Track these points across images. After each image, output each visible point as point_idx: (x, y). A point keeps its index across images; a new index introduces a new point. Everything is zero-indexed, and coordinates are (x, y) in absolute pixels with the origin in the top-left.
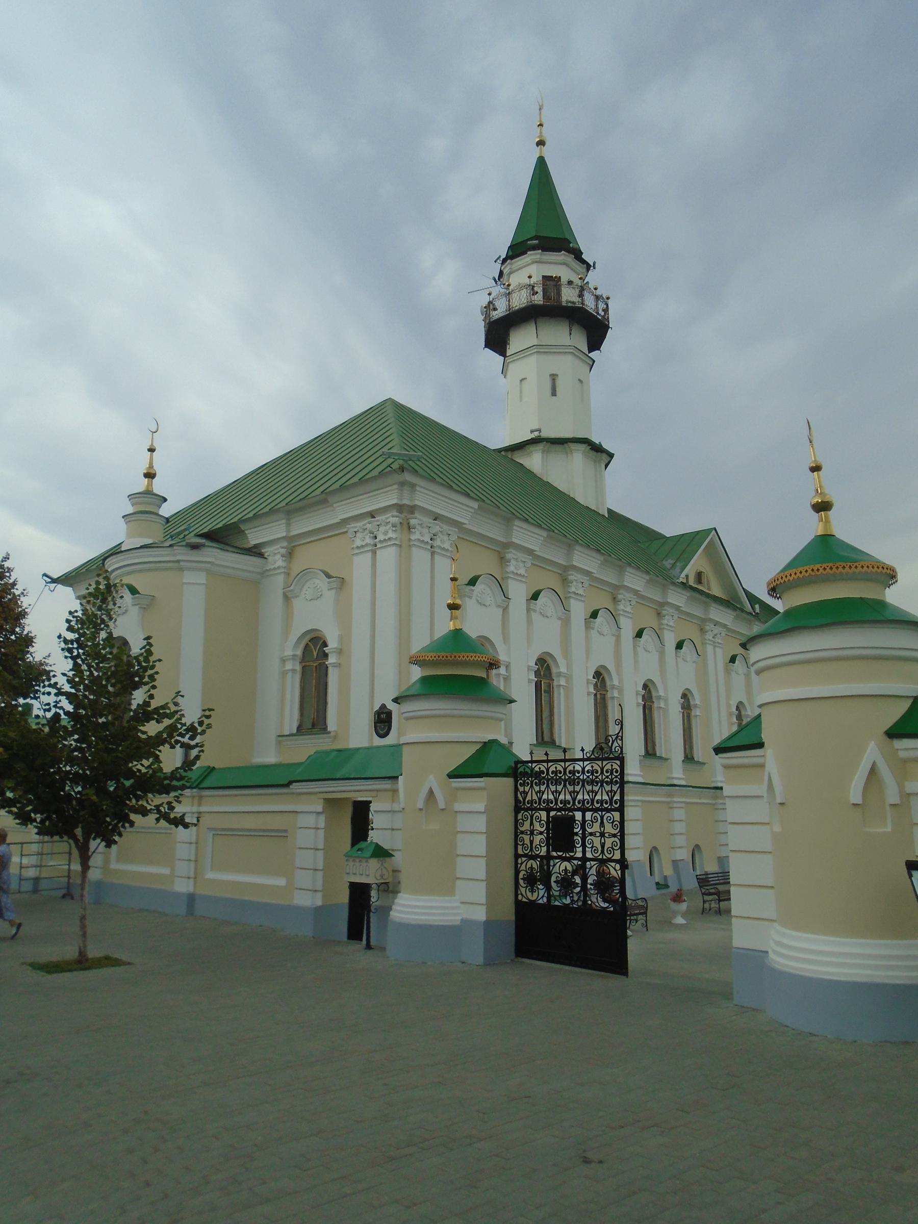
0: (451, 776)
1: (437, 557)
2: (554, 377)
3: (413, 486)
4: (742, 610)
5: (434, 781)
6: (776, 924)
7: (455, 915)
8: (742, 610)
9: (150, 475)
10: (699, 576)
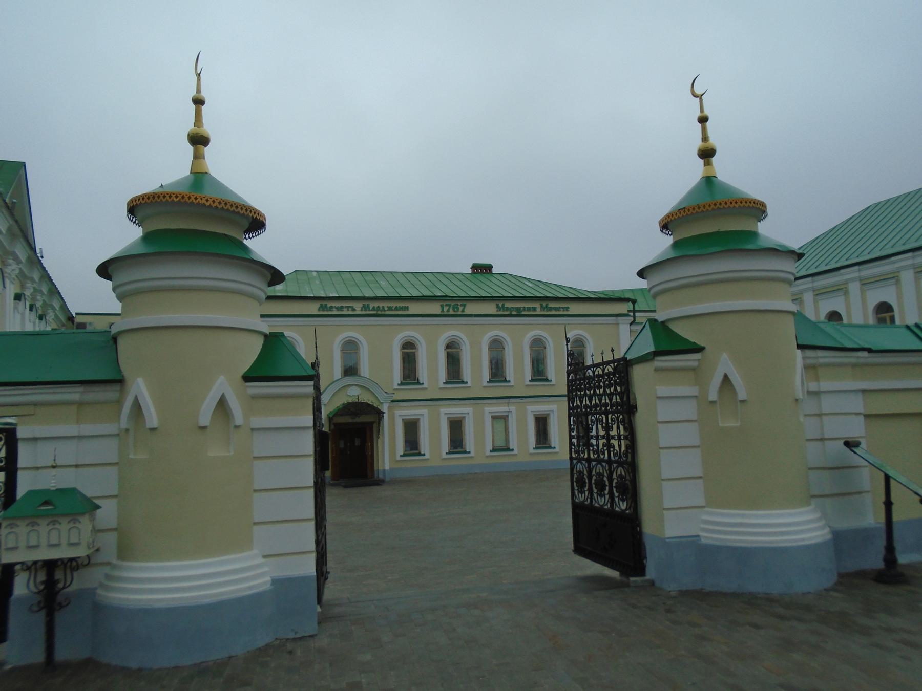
0: (247, 378)
5: (225, 385)
6: (706, 509)
7: (262, 575)
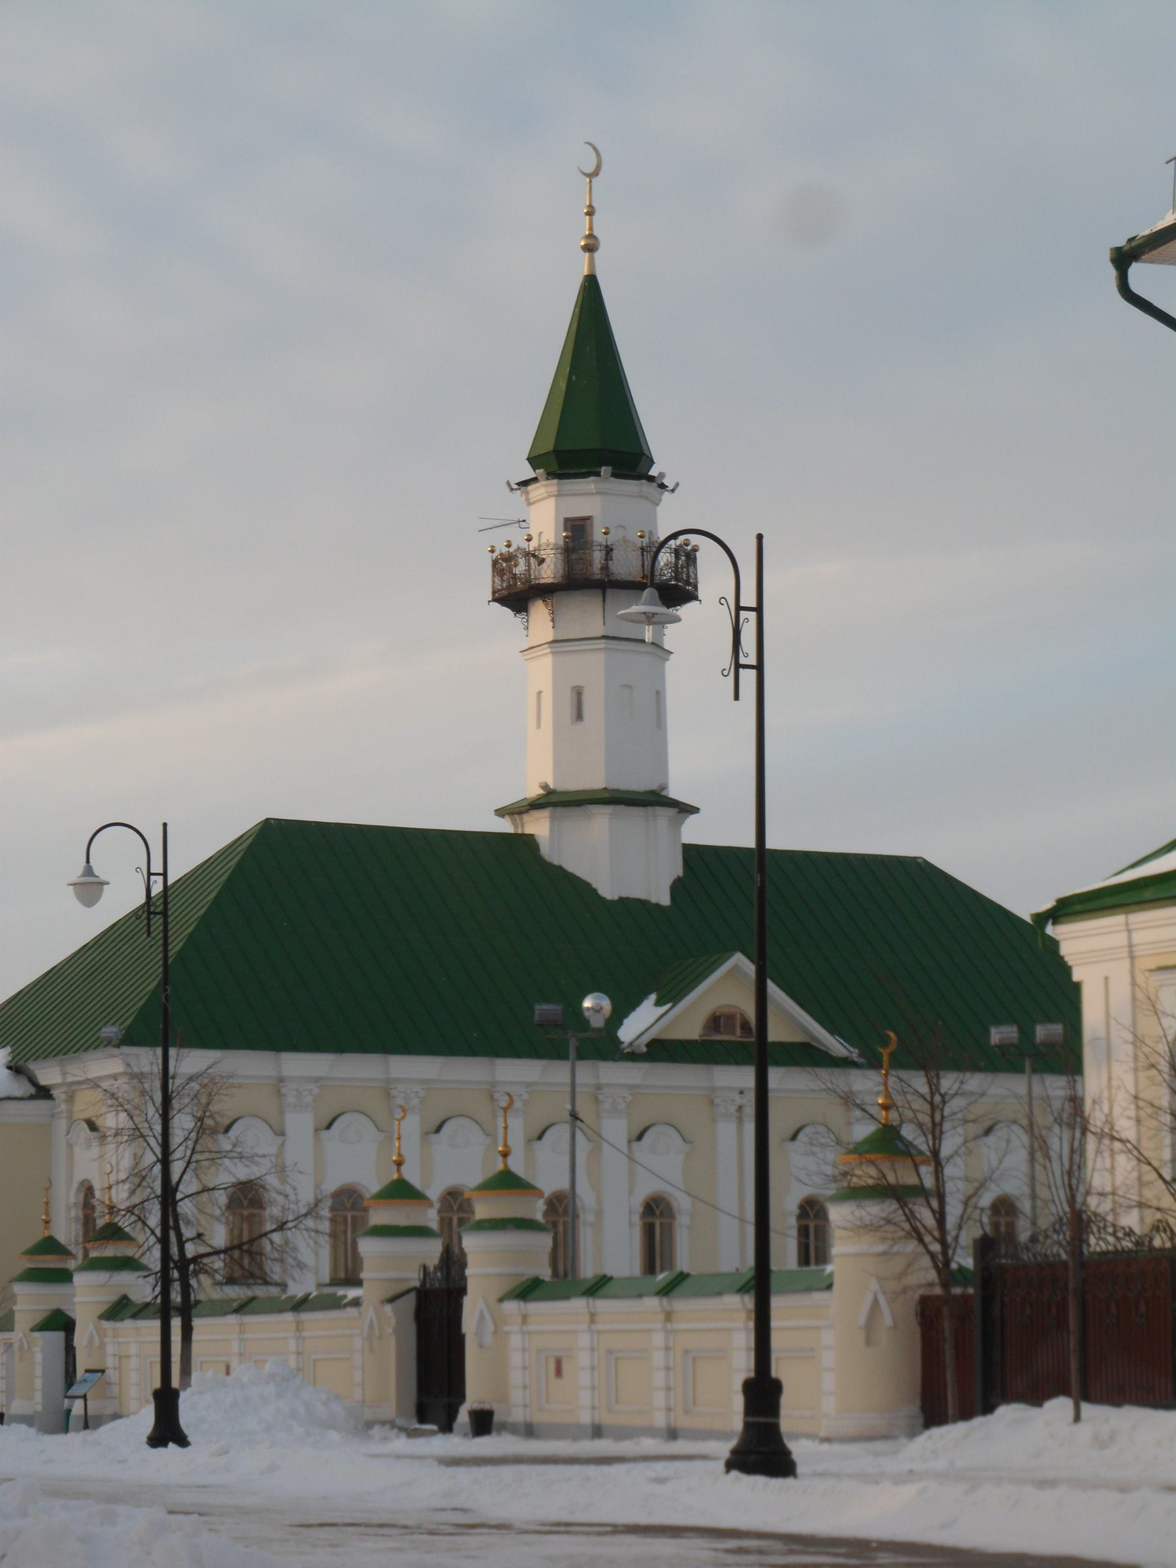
2: (578, 693)
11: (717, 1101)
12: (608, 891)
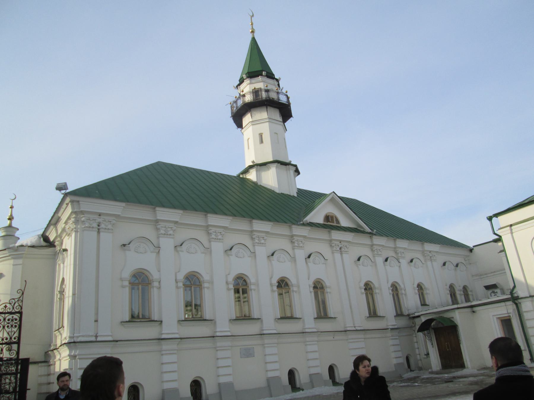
1: (101, 234)
2: (261, 135)
3: (78, 202)
4: (363, 232)
8: (363, 232)
9: (11, 219)
10: (328, 218)
11: (333, 245)
12: (278, 192)
